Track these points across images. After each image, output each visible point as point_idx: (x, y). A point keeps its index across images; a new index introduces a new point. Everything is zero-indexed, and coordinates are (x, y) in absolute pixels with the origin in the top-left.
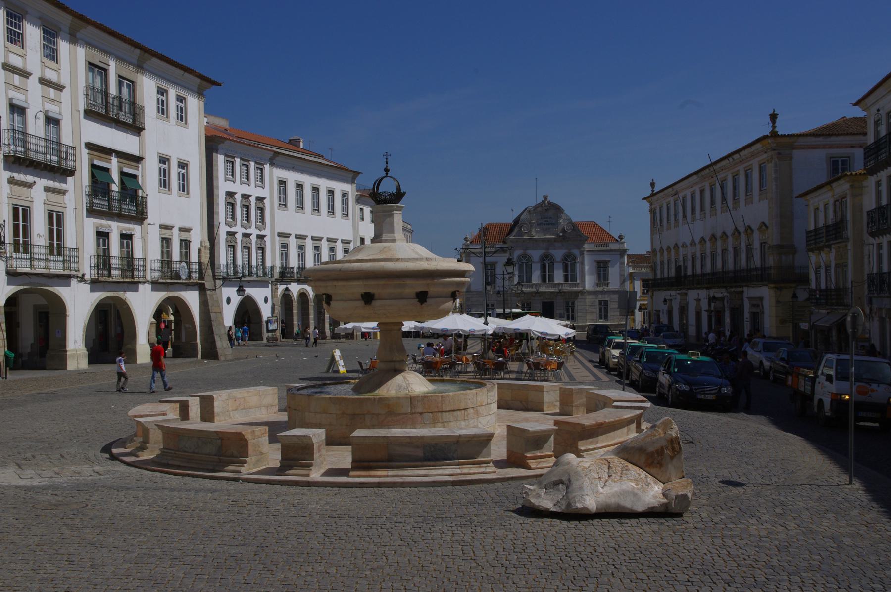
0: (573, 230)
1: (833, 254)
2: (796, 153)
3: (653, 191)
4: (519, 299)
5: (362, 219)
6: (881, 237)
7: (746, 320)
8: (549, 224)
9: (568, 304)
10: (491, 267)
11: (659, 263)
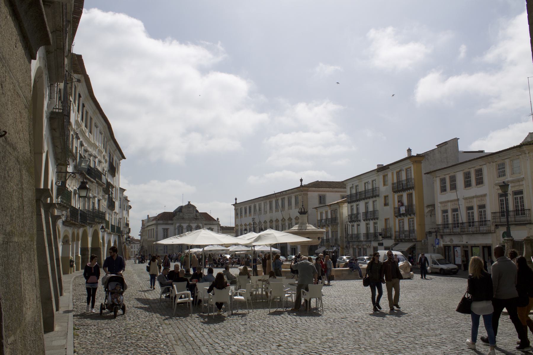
1: (330, 229)
2: (309, 193)
3: (236, 202)
5: (124, 209)
6: (353, 223)
7: (288, 251)
10: (166, 230)
11: (239, 229)
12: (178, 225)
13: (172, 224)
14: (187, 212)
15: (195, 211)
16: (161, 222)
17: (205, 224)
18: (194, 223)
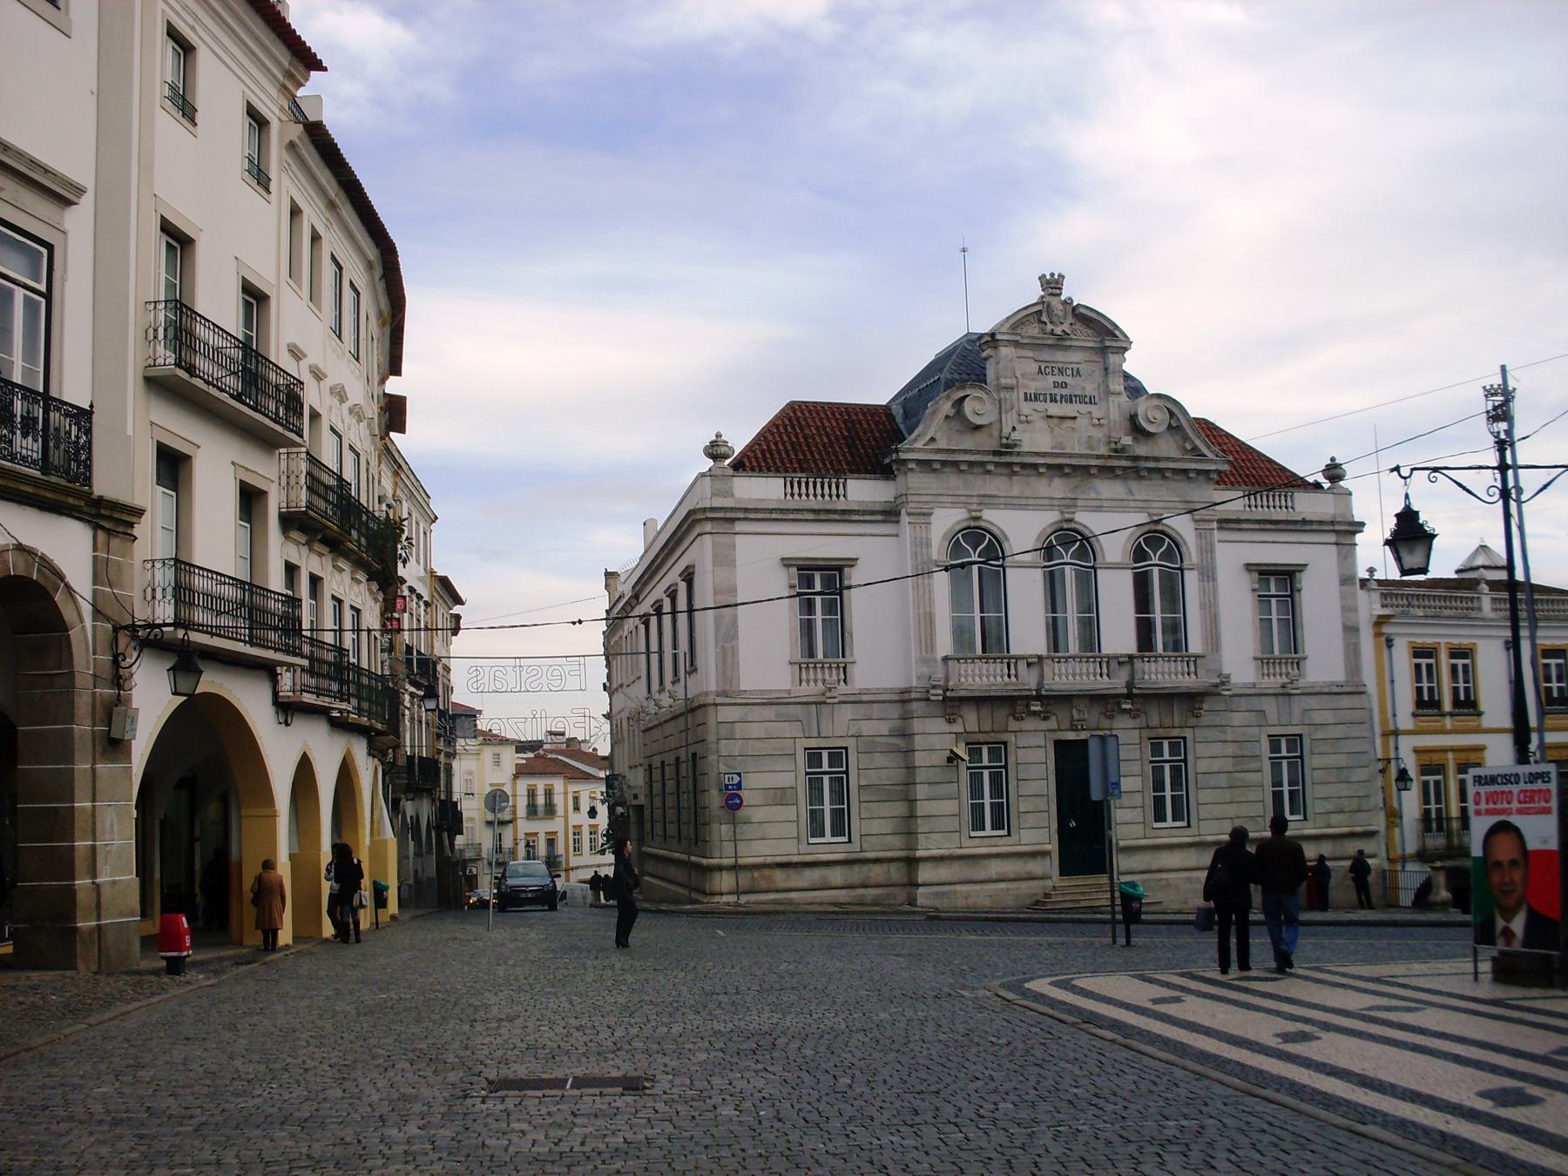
0: (1170, 427)
4: (958, 728)
8: (1069, 399)
9: (1157, 750)
10: (828, 582)
12: (946, 521)
13: (890, 514)
14: (1032, 387)
15: (1117, 385)
16: (766, 489)
17: (1225, 523)
18: (1119, 506)
